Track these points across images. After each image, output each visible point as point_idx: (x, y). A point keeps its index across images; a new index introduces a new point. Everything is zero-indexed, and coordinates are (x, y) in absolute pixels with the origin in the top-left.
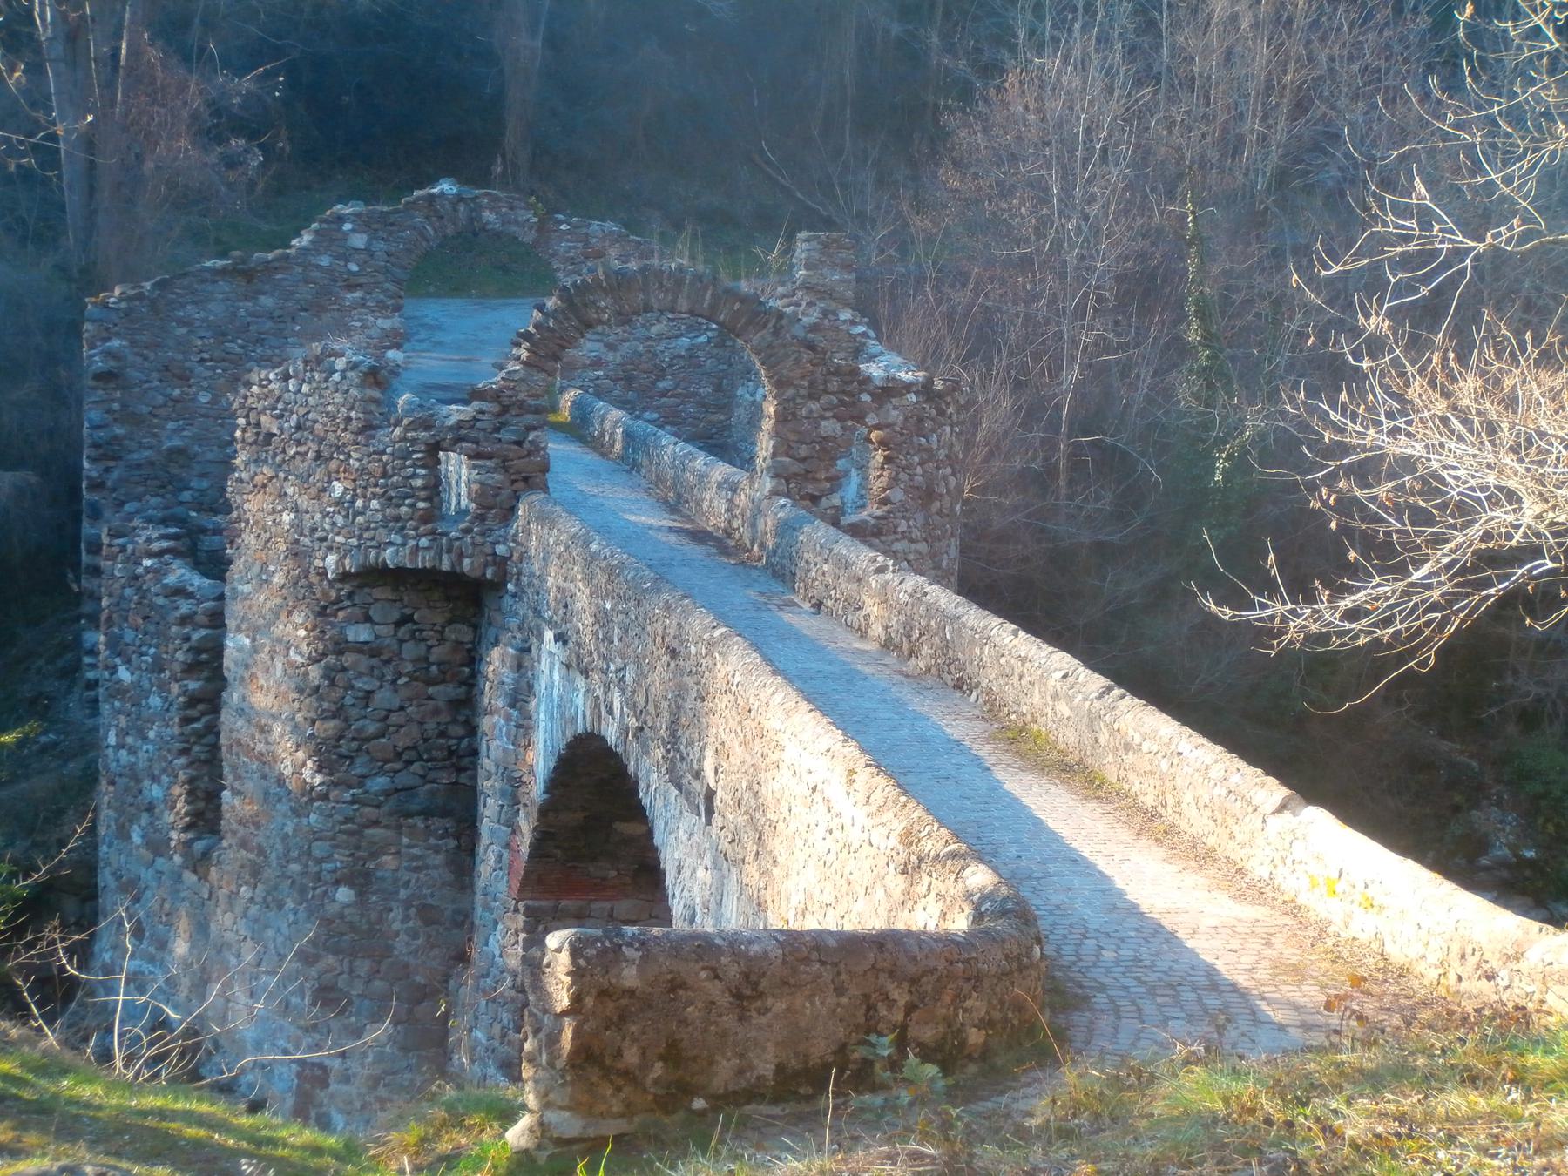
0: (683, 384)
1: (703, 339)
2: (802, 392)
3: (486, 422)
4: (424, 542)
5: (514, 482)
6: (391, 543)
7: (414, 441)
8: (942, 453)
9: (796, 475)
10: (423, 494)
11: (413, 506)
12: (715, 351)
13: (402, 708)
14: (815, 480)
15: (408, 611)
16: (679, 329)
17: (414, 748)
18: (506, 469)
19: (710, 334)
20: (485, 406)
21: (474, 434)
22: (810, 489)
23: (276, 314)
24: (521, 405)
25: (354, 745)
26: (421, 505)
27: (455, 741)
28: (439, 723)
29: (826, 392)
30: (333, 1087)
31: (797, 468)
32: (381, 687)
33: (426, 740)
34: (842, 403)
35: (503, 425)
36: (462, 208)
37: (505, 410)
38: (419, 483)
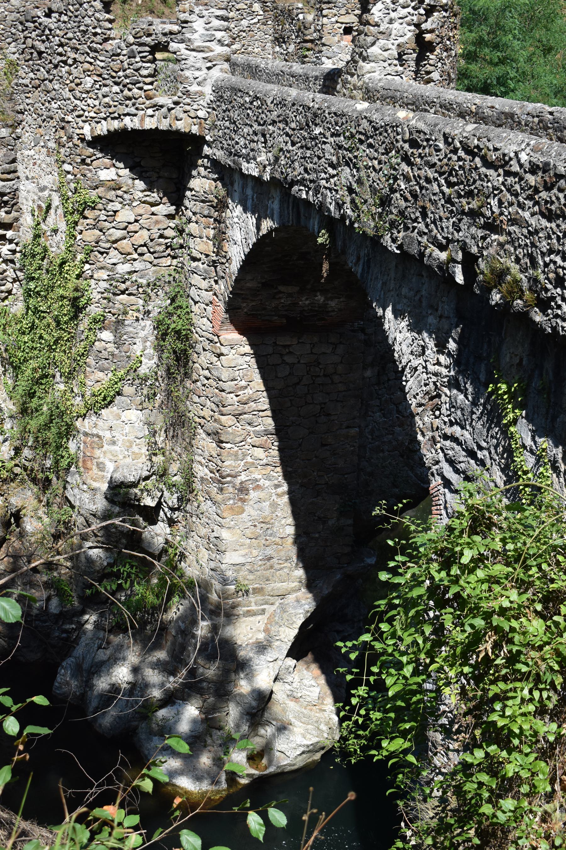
0: (246, 47)
1: (255, 20)
4: (150, 112)
6: (128, 114)
10: (149, 80)
12: (262, 27)
13: (136, 221)
15: (138, 160)
16: (242, 15)
17: (145, 245)
19: (259, 17)
23: (21, 9)
25: (108, 245)
27: (170, 240)
28: (159, 230)
30: (106, 447)
32: (122, 208)
33: (152, 240)
38: (144, 72)
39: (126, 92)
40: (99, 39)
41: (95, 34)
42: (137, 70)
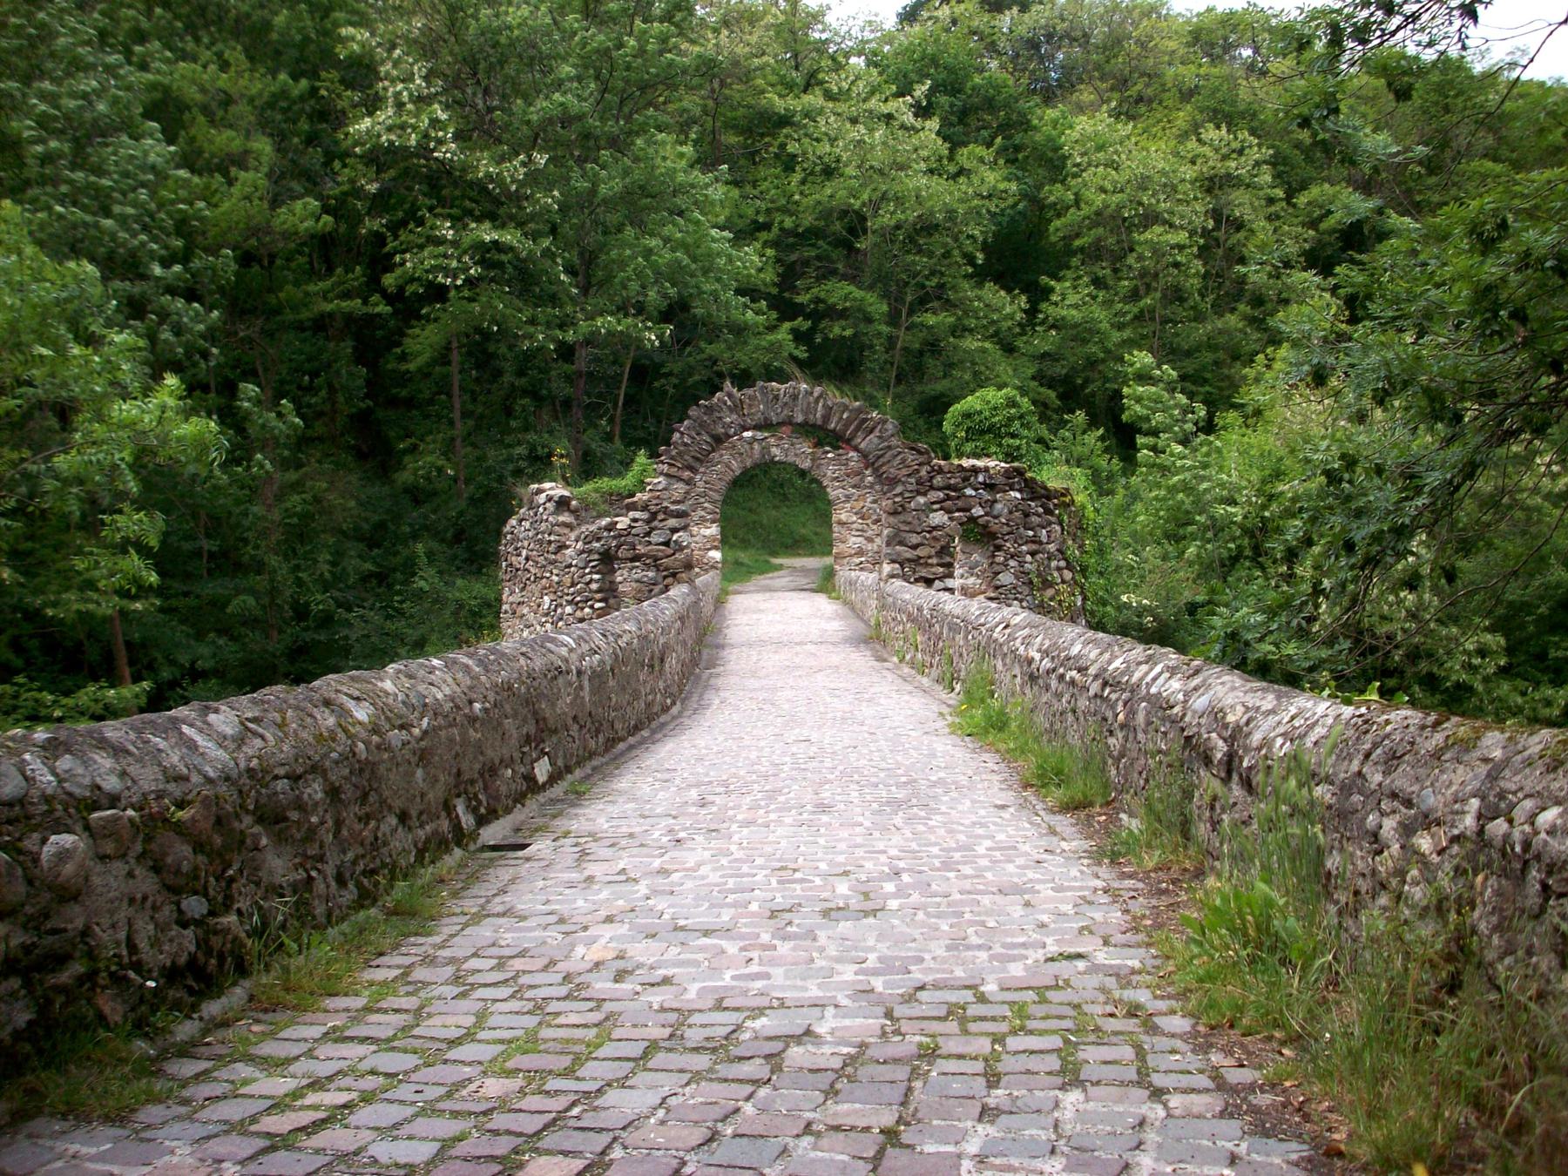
2: (910, 488)
3: (640, 528)
5: (665, 577)
7: (590, 552)
8: (1052, 547)
9: (909, 560)
10: (598, 596)
11: (592, 607)
14: (927, 565)
18: (657, 568)
20: (637, 515)
21: (630, 539)
22: (923, 573)
24: (666, 510)
26: (598, 605)
29: (932, 488)
31: (909, 554)
34: (948, 498)
35: (652, 529)
36: (756, 446)
37: (654, 516)
38: (594, 586)
39: (579, 614)
40: (552, 547)
41: (550, 542)
42: (588, 584)
